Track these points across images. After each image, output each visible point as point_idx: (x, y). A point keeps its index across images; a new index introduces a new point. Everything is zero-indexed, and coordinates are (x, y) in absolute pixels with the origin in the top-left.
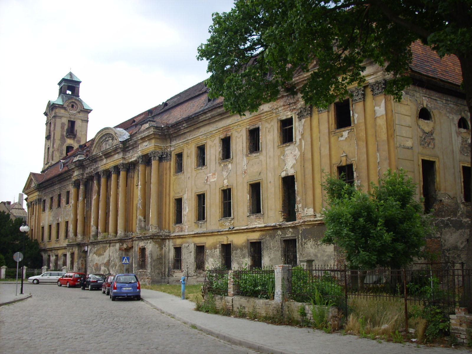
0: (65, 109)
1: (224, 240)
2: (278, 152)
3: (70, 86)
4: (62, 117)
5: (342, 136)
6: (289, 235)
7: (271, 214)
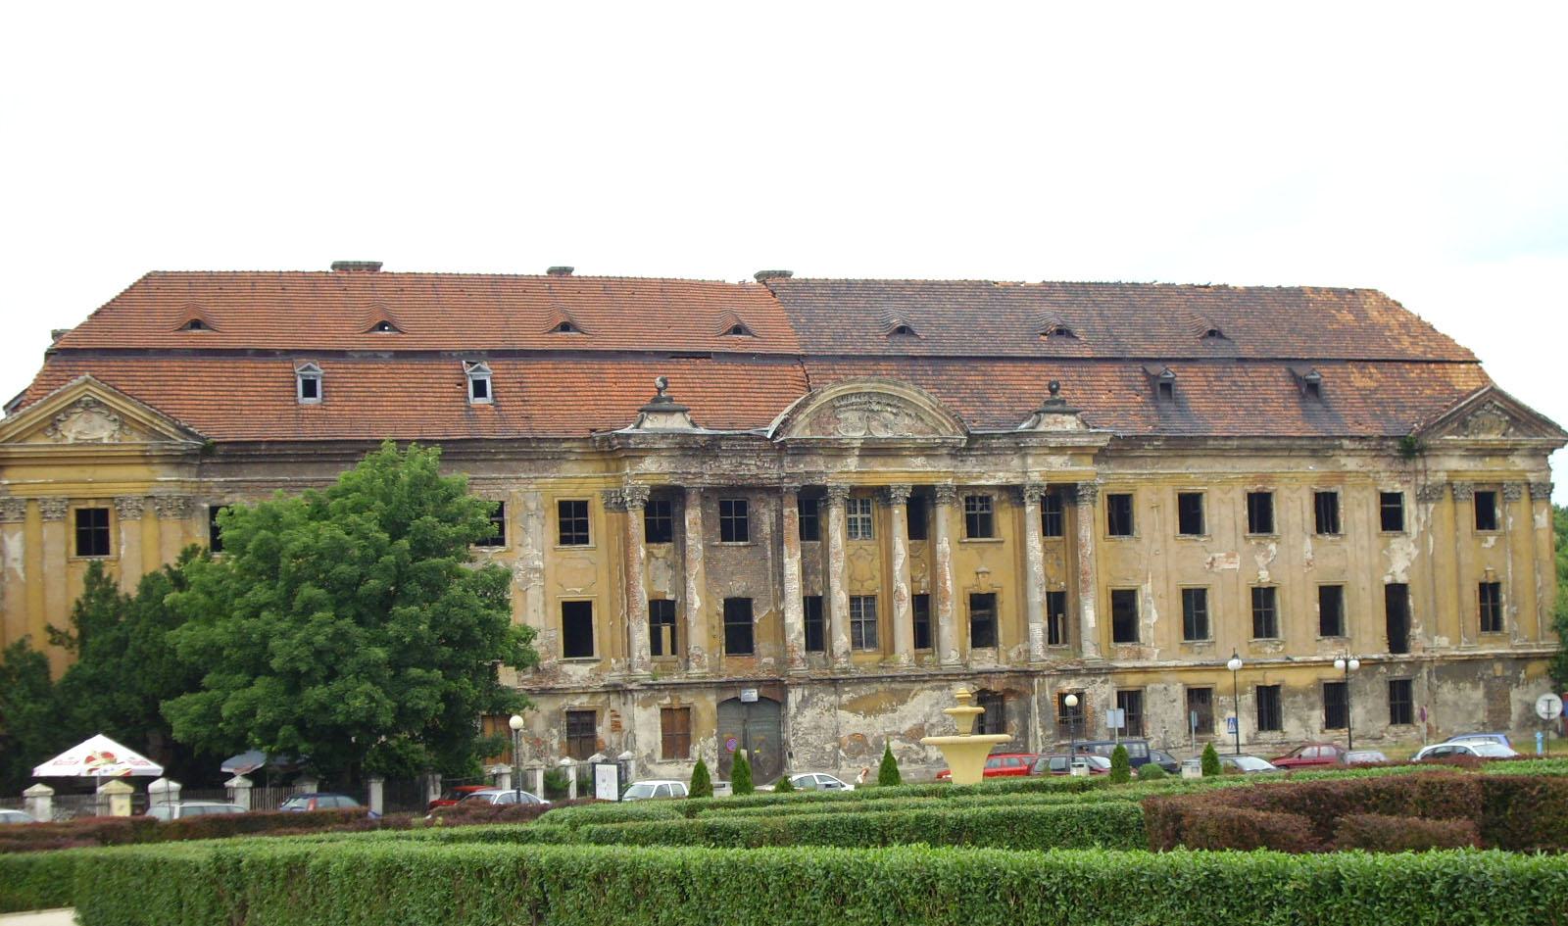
1: (1271, 679)
2: (1378, 543)
5: (1486, 542)
6: (1400, 673)
7: (1366, 639)
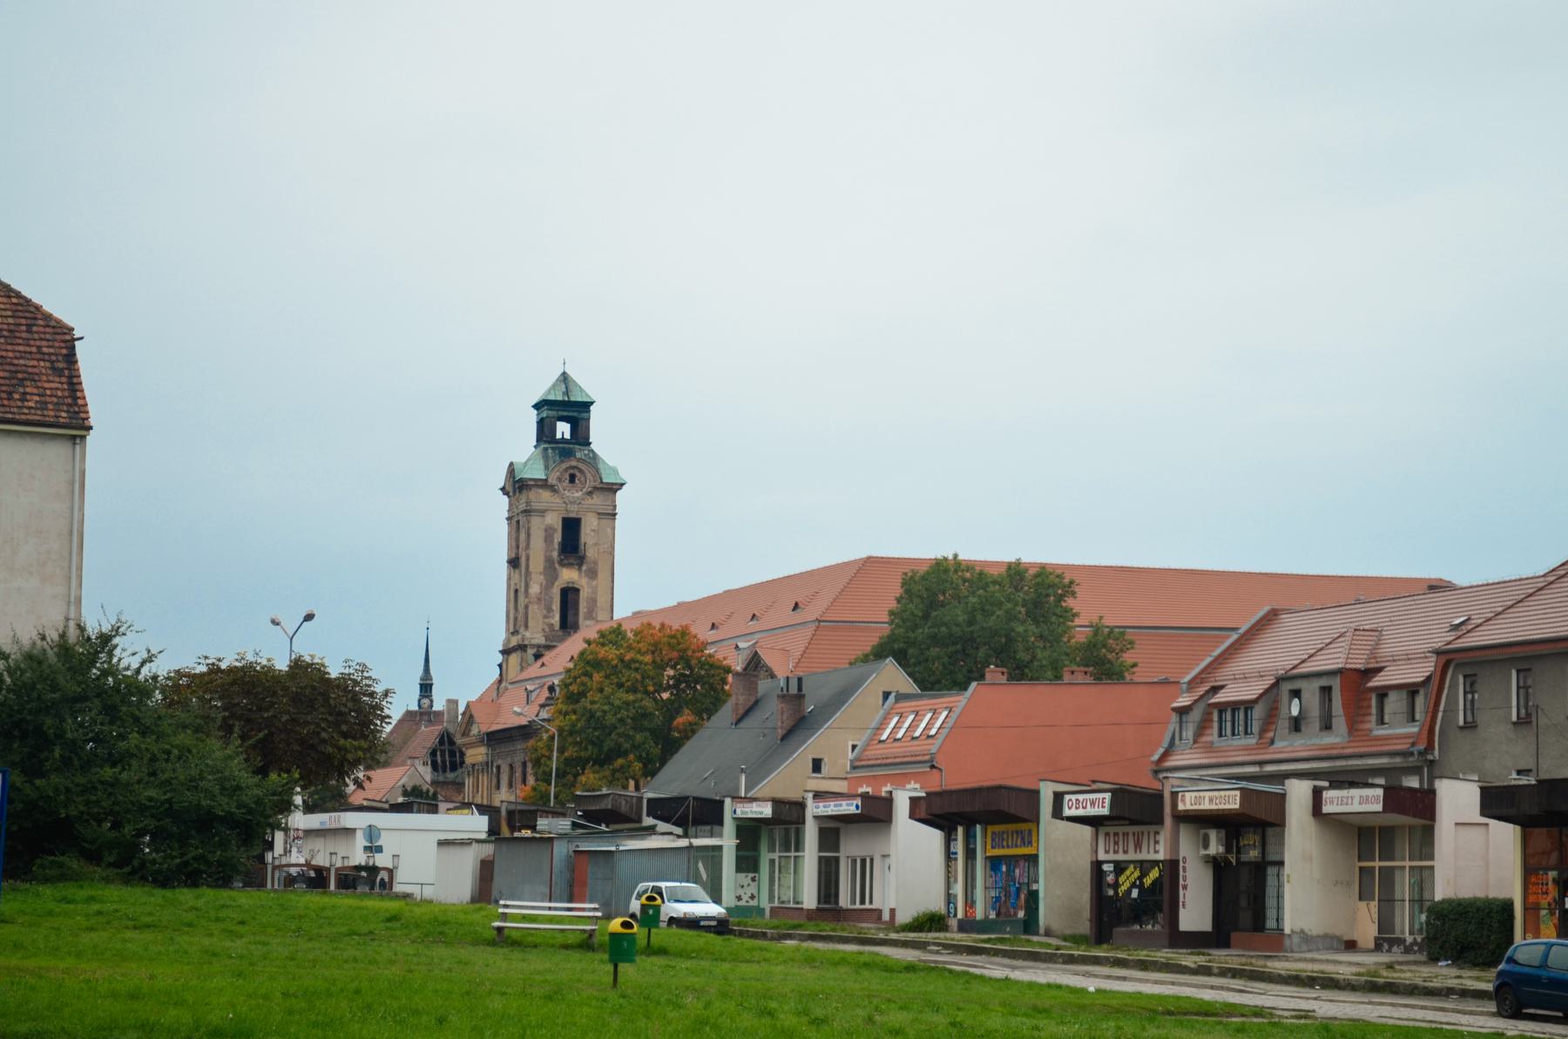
0: (552, 488)
3: (564, 415)
4: (544, 511)
